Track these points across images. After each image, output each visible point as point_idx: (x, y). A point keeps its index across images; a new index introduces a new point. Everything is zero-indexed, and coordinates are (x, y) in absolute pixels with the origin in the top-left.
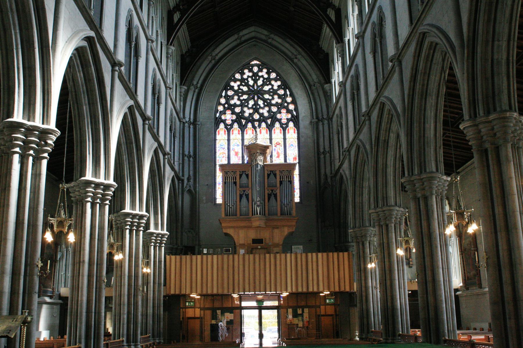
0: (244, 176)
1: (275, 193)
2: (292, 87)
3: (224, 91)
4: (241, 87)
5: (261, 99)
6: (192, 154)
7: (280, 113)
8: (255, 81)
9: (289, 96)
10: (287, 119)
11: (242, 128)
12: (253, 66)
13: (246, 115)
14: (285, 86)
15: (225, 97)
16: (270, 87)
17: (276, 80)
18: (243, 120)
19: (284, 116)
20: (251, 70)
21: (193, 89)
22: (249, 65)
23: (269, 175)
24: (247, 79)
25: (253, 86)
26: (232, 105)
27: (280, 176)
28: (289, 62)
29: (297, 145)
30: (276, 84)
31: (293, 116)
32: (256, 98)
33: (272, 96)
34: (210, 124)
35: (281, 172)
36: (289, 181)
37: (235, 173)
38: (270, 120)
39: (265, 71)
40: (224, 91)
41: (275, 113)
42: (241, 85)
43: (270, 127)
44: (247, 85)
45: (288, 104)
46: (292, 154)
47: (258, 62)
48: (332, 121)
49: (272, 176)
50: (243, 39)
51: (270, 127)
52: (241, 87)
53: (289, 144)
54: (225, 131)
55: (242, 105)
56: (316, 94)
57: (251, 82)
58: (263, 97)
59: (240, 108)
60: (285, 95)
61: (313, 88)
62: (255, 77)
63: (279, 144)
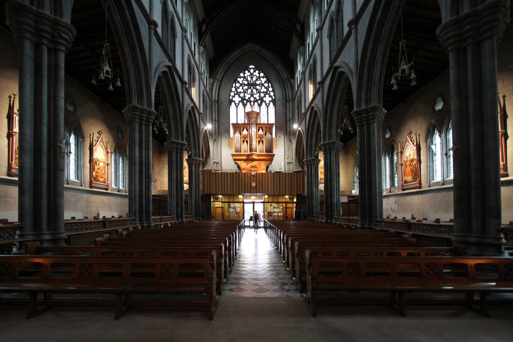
1: (262, 140)
2: (273, 82)
3: (234, 84)
5: (255, 89)
7: (265, 97)
8: (252, 78)
9: (270, 87)
11: (245, 105)
12: (250, 69)
13: (247, 98)
14: (268, 81)
15: (234, 87)
17: (263, 77)
18: (244, 101)
19: (267, 99)
20: (249, 72)
21: (217, 82)
25: (250, 81)
31: (272, 99)
32: (252, 88)
34: (227, 103)
35: (266, 128)
36: (270, 134)
40: (234, 84)
41: (263, 98)
43: (260, 105)
44: (247, 80)
45: (270, 92)
48: (294, 102)
51: (260, 105)
55: (244, 92)
56: (286, 86)
57: (249, 79)
58: (256, 87)
60: (269, 87)
61: (285, 82)
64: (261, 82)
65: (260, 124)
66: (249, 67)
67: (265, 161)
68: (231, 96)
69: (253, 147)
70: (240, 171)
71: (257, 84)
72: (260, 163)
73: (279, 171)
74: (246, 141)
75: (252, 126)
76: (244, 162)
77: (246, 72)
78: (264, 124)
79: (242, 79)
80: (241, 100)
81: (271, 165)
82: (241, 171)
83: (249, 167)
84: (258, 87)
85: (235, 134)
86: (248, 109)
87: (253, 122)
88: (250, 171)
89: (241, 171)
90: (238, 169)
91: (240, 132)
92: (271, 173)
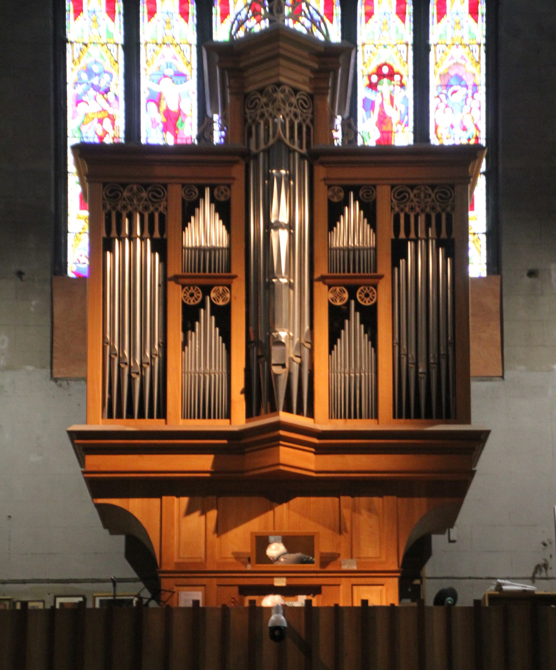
1: (367, 303)
29: (481, 79)
36: (439, 243)
46: (458, 130)
53: (442, 76)
63: (391, 75)
67: (390, 500)
69: (276, 370)
70: (147, 594)
72: (346, 513)
73: (530, 587)
75: (269, 177)
76: (189, 511)
81: (454, 533)
82: (156, 592)
83: (238, 556)
85: (108, 246)
87: (280, 141)
88: (245, 590)
89: (156, 592)
90: (133, 575)
92: (450, 610)
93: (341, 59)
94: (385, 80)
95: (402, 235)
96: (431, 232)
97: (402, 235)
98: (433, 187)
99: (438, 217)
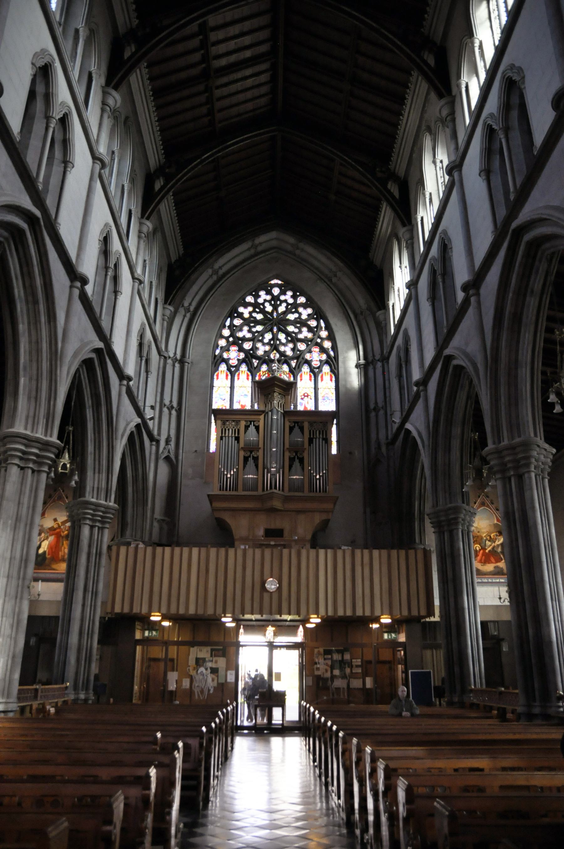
0: (252, 428)
1: (301, 456)
3: (229, 319)
4: (254, 315)
5: (283, 332)
6: (175, 404)
8: (275, 307)
10: (321, 361)
11: (253, 371)
13: (260, 352)
14: (319, 314)
15: (229, 327)
16: (296, 315)
17: (305, 306)
18: (254, 361)
20: (269, 292)
22: (265, 285)
23: (291, 429)
24: (263, 304)
26: (239, 339)
27: (310, 431)
28: (325, 282)
29: (334, 397)
30: (305, 313)
31: (329, 356)
32: (275, 330)
33: (300, 329)
34: (206, 363)
35: (311, 424)
36: (323, 439)
37: (237, 422)
38: (295, 361)
39: (290, 293)
42: (254, 311)
47: (280, 282)
48: (388, 363)
49: (297, 430)
50: (260, 249)
52: (254, 315)
54: (227, 375)
58: (286, 329)
59: (251, 343)
60: (318, 326)
61: (361, 317)
62: (275, 302)
63: (307, 396)
64: (300, 317)
65: (297, 413)
66: (270, 282)
68: (219, 348)
71: (288, 320)
74: (254, 458)
77: (262, 293)
78: (306, 413)
79: (250, 309)
80: (246, 356)
84: (291, 328)
86: (263, 372)
91: (238, 434)
93: (294, 386)
94: (306, 397)
95: (312, 436)
96: (321, 436)
97: (312, 436)
98: (321, 423)
99: (323, 431)
